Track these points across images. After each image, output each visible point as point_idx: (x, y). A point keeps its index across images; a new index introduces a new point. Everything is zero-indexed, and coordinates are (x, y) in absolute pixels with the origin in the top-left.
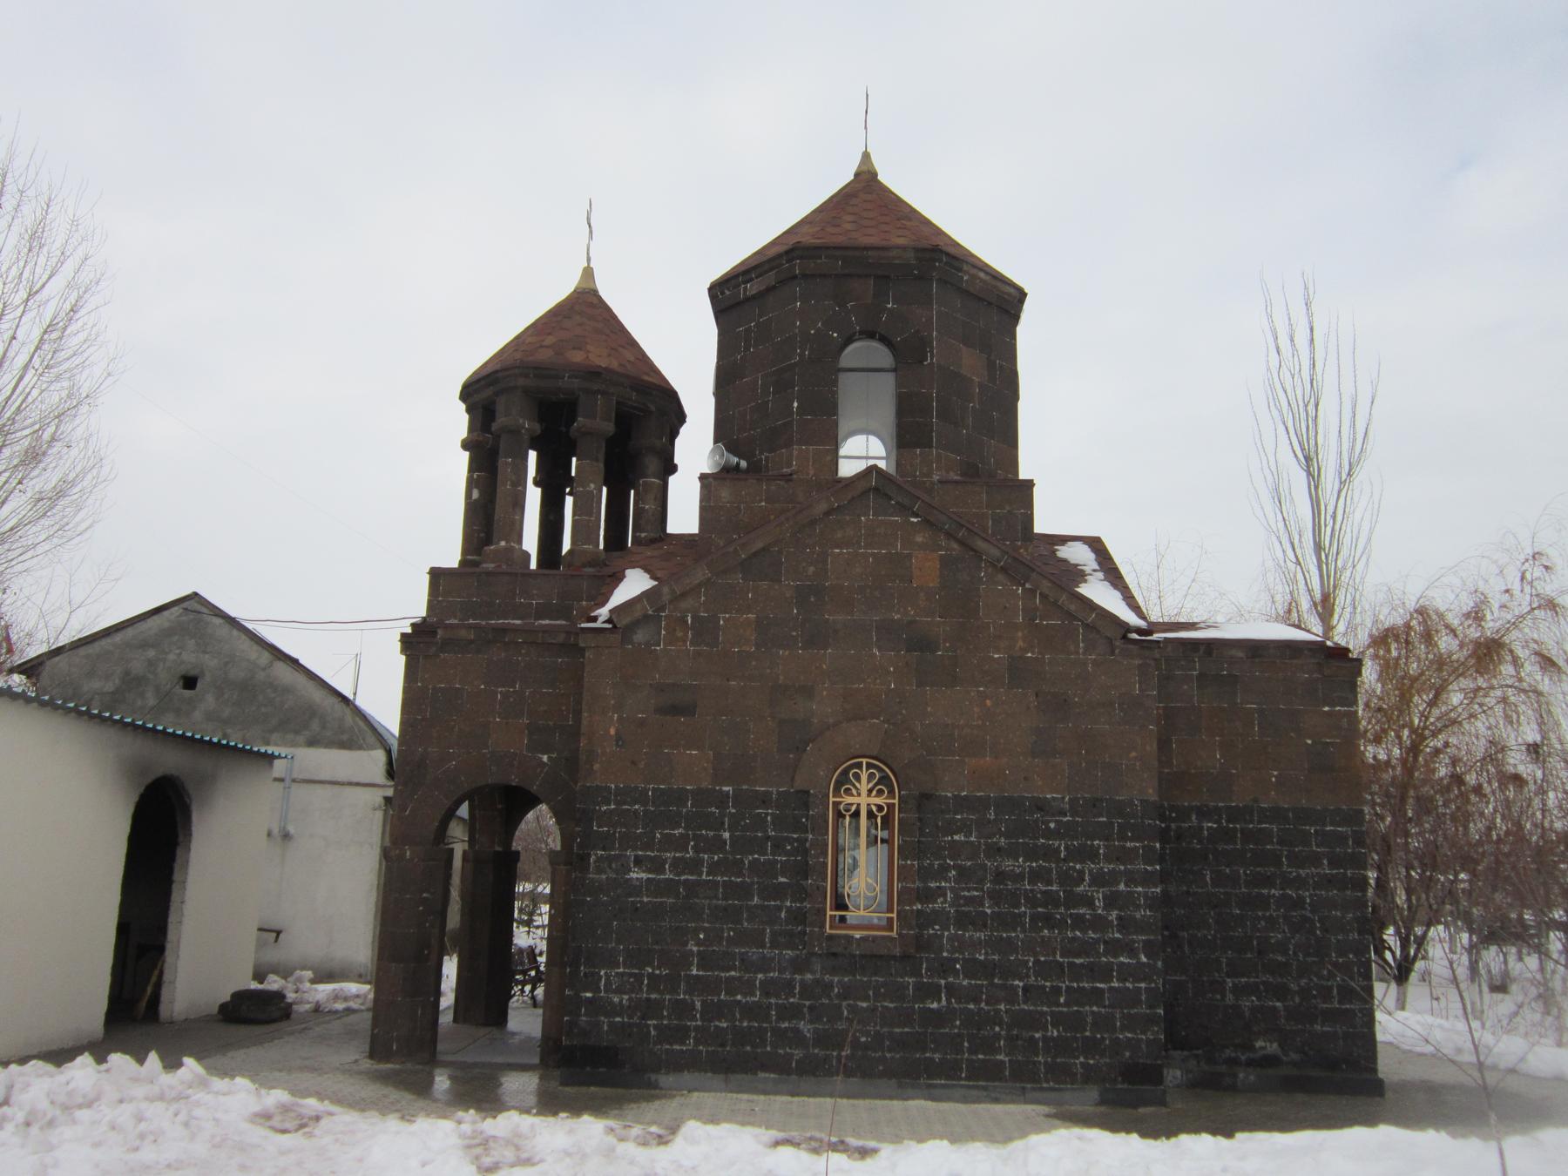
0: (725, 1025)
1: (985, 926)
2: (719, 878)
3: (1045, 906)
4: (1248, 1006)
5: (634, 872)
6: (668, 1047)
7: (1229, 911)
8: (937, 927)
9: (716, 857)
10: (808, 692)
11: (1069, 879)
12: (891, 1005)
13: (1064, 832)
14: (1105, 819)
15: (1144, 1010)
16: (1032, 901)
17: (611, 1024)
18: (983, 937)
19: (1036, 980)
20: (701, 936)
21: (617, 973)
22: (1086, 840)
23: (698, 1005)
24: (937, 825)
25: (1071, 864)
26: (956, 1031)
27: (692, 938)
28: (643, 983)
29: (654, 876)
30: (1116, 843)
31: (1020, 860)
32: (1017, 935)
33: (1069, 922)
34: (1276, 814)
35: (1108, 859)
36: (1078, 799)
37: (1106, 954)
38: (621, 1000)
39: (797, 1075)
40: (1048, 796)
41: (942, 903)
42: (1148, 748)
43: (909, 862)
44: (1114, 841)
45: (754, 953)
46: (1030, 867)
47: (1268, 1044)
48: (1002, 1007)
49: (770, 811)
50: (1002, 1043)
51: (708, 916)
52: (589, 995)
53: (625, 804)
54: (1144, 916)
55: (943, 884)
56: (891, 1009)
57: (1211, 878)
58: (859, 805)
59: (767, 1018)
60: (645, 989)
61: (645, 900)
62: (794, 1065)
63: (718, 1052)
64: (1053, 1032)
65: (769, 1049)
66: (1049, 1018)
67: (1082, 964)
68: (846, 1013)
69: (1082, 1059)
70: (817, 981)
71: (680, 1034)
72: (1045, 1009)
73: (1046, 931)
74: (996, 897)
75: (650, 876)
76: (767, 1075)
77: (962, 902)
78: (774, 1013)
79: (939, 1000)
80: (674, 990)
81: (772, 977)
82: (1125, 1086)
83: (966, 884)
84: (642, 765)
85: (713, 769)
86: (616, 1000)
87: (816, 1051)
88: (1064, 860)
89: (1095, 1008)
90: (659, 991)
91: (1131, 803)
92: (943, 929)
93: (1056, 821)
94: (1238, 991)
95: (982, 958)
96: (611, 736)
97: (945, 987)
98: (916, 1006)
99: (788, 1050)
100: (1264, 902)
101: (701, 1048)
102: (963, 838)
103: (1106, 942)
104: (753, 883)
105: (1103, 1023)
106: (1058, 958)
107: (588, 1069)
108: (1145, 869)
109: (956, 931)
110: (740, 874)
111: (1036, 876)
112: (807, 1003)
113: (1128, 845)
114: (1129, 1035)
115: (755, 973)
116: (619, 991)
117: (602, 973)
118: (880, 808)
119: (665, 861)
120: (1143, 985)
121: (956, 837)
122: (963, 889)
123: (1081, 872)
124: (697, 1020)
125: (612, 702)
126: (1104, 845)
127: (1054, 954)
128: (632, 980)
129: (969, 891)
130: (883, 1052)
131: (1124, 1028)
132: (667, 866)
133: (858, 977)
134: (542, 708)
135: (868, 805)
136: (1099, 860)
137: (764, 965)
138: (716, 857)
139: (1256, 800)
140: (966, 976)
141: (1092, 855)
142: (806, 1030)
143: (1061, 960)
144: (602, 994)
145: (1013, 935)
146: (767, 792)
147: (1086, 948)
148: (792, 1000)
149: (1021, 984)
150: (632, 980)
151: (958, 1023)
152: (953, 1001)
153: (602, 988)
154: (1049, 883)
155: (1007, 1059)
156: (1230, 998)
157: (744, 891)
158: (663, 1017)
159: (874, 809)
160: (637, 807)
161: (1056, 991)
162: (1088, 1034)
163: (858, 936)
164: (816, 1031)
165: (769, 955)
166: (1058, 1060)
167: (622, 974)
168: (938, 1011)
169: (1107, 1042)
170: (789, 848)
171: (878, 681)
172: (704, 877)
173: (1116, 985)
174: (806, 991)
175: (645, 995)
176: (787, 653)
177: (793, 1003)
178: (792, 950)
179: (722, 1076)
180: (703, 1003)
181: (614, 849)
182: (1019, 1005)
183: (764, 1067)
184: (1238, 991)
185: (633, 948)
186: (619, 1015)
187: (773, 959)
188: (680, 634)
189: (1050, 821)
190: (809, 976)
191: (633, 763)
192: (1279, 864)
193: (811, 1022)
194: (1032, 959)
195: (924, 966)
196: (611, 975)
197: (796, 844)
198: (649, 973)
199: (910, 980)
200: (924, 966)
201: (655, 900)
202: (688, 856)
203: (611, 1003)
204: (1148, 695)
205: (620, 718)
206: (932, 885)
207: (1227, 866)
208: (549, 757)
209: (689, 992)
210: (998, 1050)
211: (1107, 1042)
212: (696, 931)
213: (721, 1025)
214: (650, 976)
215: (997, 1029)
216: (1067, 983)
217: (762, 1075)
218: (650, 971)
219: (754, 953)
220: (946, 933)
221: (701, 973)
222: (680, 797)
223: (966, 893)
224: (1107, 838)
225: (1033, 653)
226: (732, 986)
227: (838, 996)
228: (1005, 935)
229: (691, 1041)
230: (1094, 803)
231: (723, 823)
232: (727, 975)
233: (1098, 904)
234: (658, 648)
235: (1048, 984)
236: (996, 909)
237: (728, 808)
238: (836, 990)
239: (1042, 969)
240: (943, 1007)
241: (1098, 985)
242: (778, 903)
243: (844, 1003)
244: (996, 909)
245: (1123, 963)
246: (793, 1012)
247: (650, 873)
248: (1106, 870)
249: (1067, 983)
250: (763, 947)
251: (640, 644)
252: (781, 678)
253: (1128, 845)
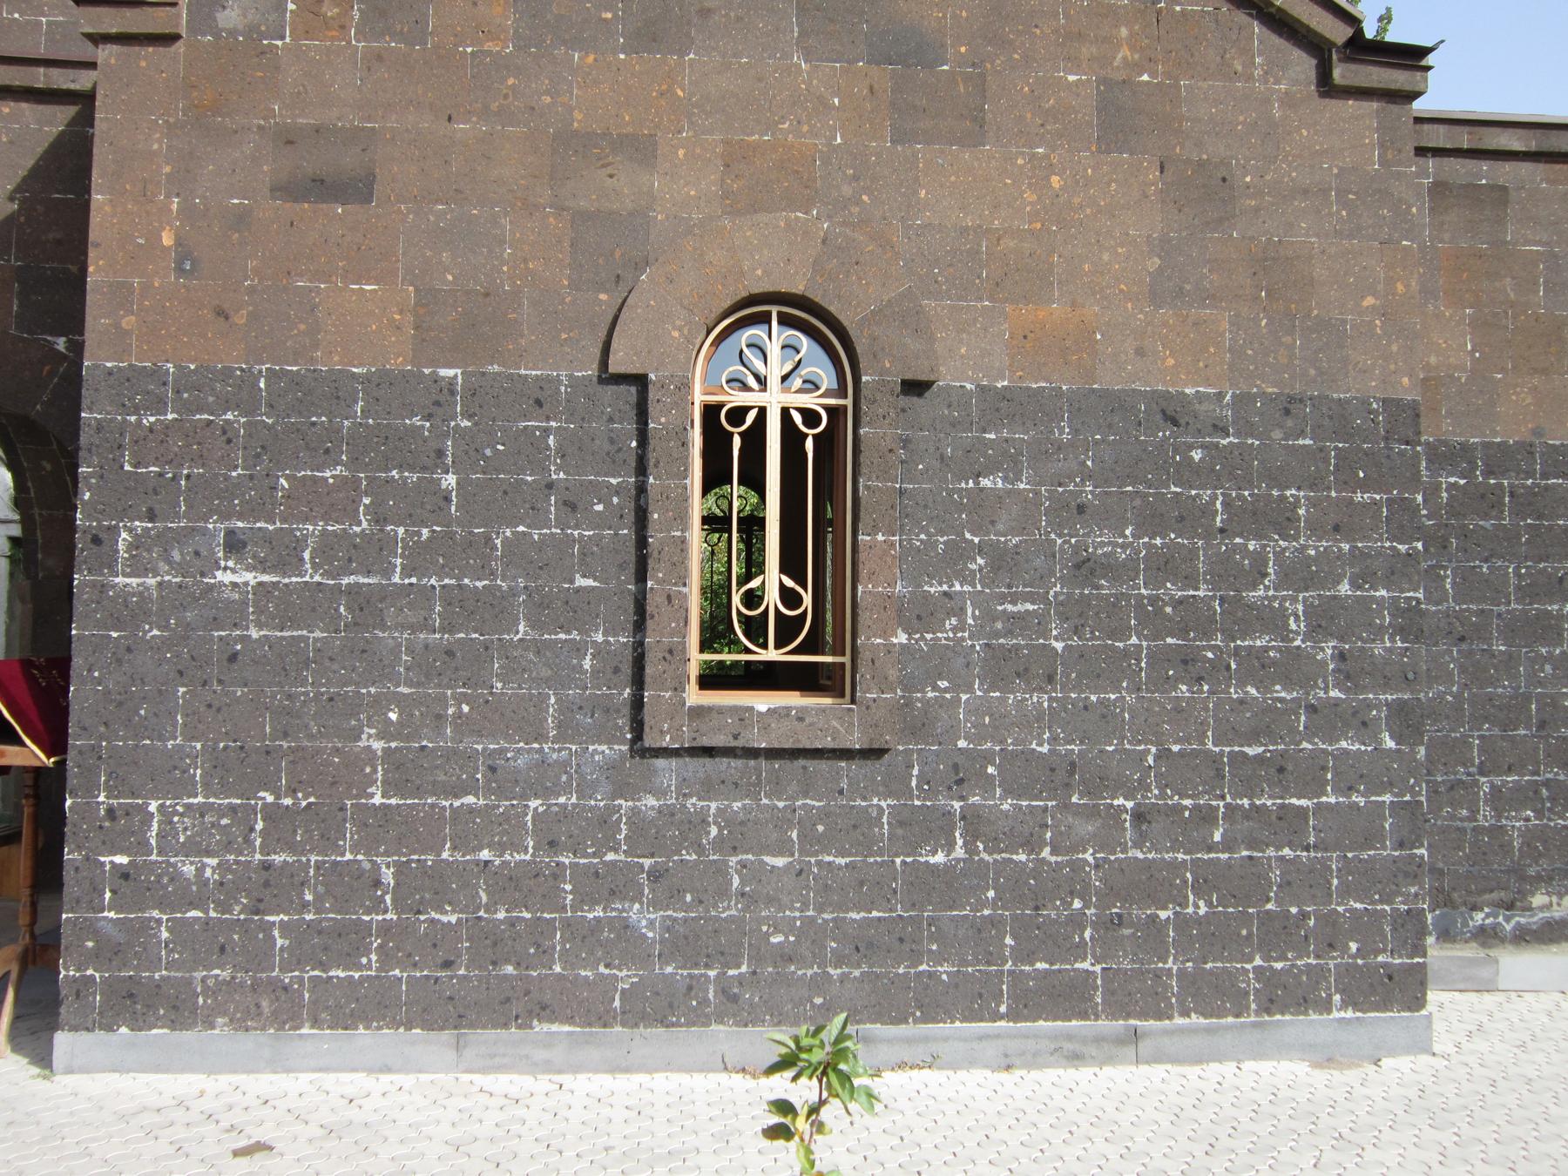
0: (453, 919)
1: (1050, 679)
2: (433, 581)
3: (1182, 632)
4: (1519, 829)
5: (226, 568)
6: (316, 973)
7: (1485, 647)
8: (943, 684)
9: (425, 532)
10: (642, 150)
12: (842, 861)
13: (1225, 468)
14: (1308, 442)
15: (1389, 852)
16: (1152, 620)
17: (177, 927)
18: (1046, 704)
19: (1162, 796)
20: (393, 716)
21: (188, 807)
22: (1270, 487)
23: (388, 876)
24: (942, 457)
25: (1238, 540)
26: (986, 912)
27: (369, 719)
28: (252, 829)
29: (275, 579)
30: (1333, 494)
31: (1128, 532)
32: (1121, 696)
33: (1233, 666)
35: (1315, 529)
36: (1251, 398)
37: (1310, 731)
38: (200, 870)
39: (623, 1025)
40: (1187, 391)
41: (955, 629)
42: (1400, 287)
43: (880, 537)
44: (1329, 489)
45: (520, 754)
46: (1148, 546)
47: (1555, 899)
48: (1088, 857)
49: (553, 424)
50: (1087, 934)
51: (407, 669)
52: (122, 859)
53: (200, 410)
54: (1389, 650)
55: (958, 587)
56: (840, 867)
57: (1454, 584)
58: (762, 412)
59: (552, 899)
60: (258, 842)
61: (254, 633)
62: (617, 1003)
63: (437, 980)
64: (1197, 906)
65: (558, 969)
66: (1188, 875)
67: (1259, 759)
68: (736, 882)
69: (1258, 961)
70: (667, 813)
72: (1180, 856)
73: (1184, 688)
74: (1075, 615)
75: (266, 578)
76: (555, 1027)
77: (999, 625)
78: (568, 887)
79: (950, 846)
80: (329, 842)
81: (564, 806)
82: (1349, 1014)
83: (1010, 586)
84: (240, 319)
85: (416, 328)
86: (189, 870)
87: (669, 970)
88: (1222, 531)
89: (1286, 851)
90: (292, 847)
91: (1365, 402)
92: (956, 688)
93: (1203, 446)
95: (1045, 749)
96: (166, 249)
97: (963, 818)
98: (898, 861)
99: (602, 969)
101: (397, 972)
102: (1000, 485)
103: (1312, 709)
104: (513, 592)
106: (1210, 745)
107: (124, 1030)
108: (1393, 548)
109: (986, 691)
110: (484, 571)
111: (1164, 566)
112: (647, 862)
113: (1358, 497)
114: (1358, 906)
115: (524, 797)
116: (194, 849)
117: (153, 806)
118: (810, 417)
119: (300, 544)
120: (1387, 798)
121: (986, 482)
122: (1003, 599)
123: (1259, 560)
124: (386, 911)
125: (167, 169)
126: (1307, 498)
127: (1201, 739)
128: (225, 821)
129: (1014, 603)
130: (822, 965)
131: (1346, 892)
132: (307, 555)
133: (765, 801)
134: (51, 236)
135: (785, 412)
136: (1297, 529)
137: (543, 780)
138: (425, 532)
139: (1537, 432)
140: (1008, 792)
141: (1283, 522)
142: (644, 923)
143: (1217, 749)
144: (154, 857)
145: (1113, 697)
146: (548, 379)
147: (1267, 724)
148: (610, 857)
149: (1130, 805)
150: (225, 821)
151: (991, 894)
152: (981, 847)
153: (153, 842)
154: (1191, 581)
155: (1098, 968)
156: (1485, 816)
157: (495, 609)
158: (305, 906)
159: (797, 418)
160: (229, 416)
161: (1206, 817)
162: (1269, 906)
163: (763, 708)
164: (669, 926)
165: (555, 756)
166: (1209, 966)
167: (203, 810)
168: (948, 868)
169: (1312, 923)
170: (599, 508)
171: (805, 128)
172: (396, 579)
173: (1332, 800)
174: (645, 835)
175: (258, 856)
176: (591, 58)
177: (614, 863)
178: (609, 742)
179: (447, 1035)
180: (401, 870)
181: (177, 516)
182: (1124, 851)
183: (545, 1011)
185: (226, 748)
186: (192, 905)
187: (564, 765)
188: (332, 12)
189: (1191, 447)
190: (651, 801)
191: (222, 314)
193: (655, 904)
194: (1153, 750)
195: (915, 772)
196: (176, 813)
197: (615, 500)
198: (265, 805)
199: (883, 804)
200: (915, 772)
201: (279, 634)
202: (357, 529)
203: (176, 877)
204: (1399, 173)
205: (187, 211)
206: (932, 590)
207: (1486, 560)
208: (69, 341)
209: (367, 844)
210: (1079, 951)
211: (1312, 923)
212: (378, 705)
213: (445, 919)
214: (271, 813)
215: (1077, 904)
216: (1228, 799)
217: (540, 1027)
218: (270, 799)
219: (520, 754)
220: (964, 697)
221: (393, 801)
222: (337, 391)
223: (1010, 607)
225: (1153, 74)
226: (467, 830)
227: (719, 843)
228: (1093, 698)
229: (374, 957)
230: (1288, 405)
231: (440, 453)
232: (457, 804)
233: (1293, 626)
234: (279, 43)
235: (1187, 802)
236: (1075, 641)
237: (454, 418)
238: (714, 831)
239: (1176, 770)
240: (958, 860)
241: (1294, 801)
242: (575, 635)
243: (733, 861)
244: (1075, 641)
245: (1346, 752)
246: (614, 885)
247: (264, 571)
248: (1312, 553)
249: (1228, 799)
250: (541, 737)
251: (233, 33)
252: (577, 115)
253: (1358, 497)
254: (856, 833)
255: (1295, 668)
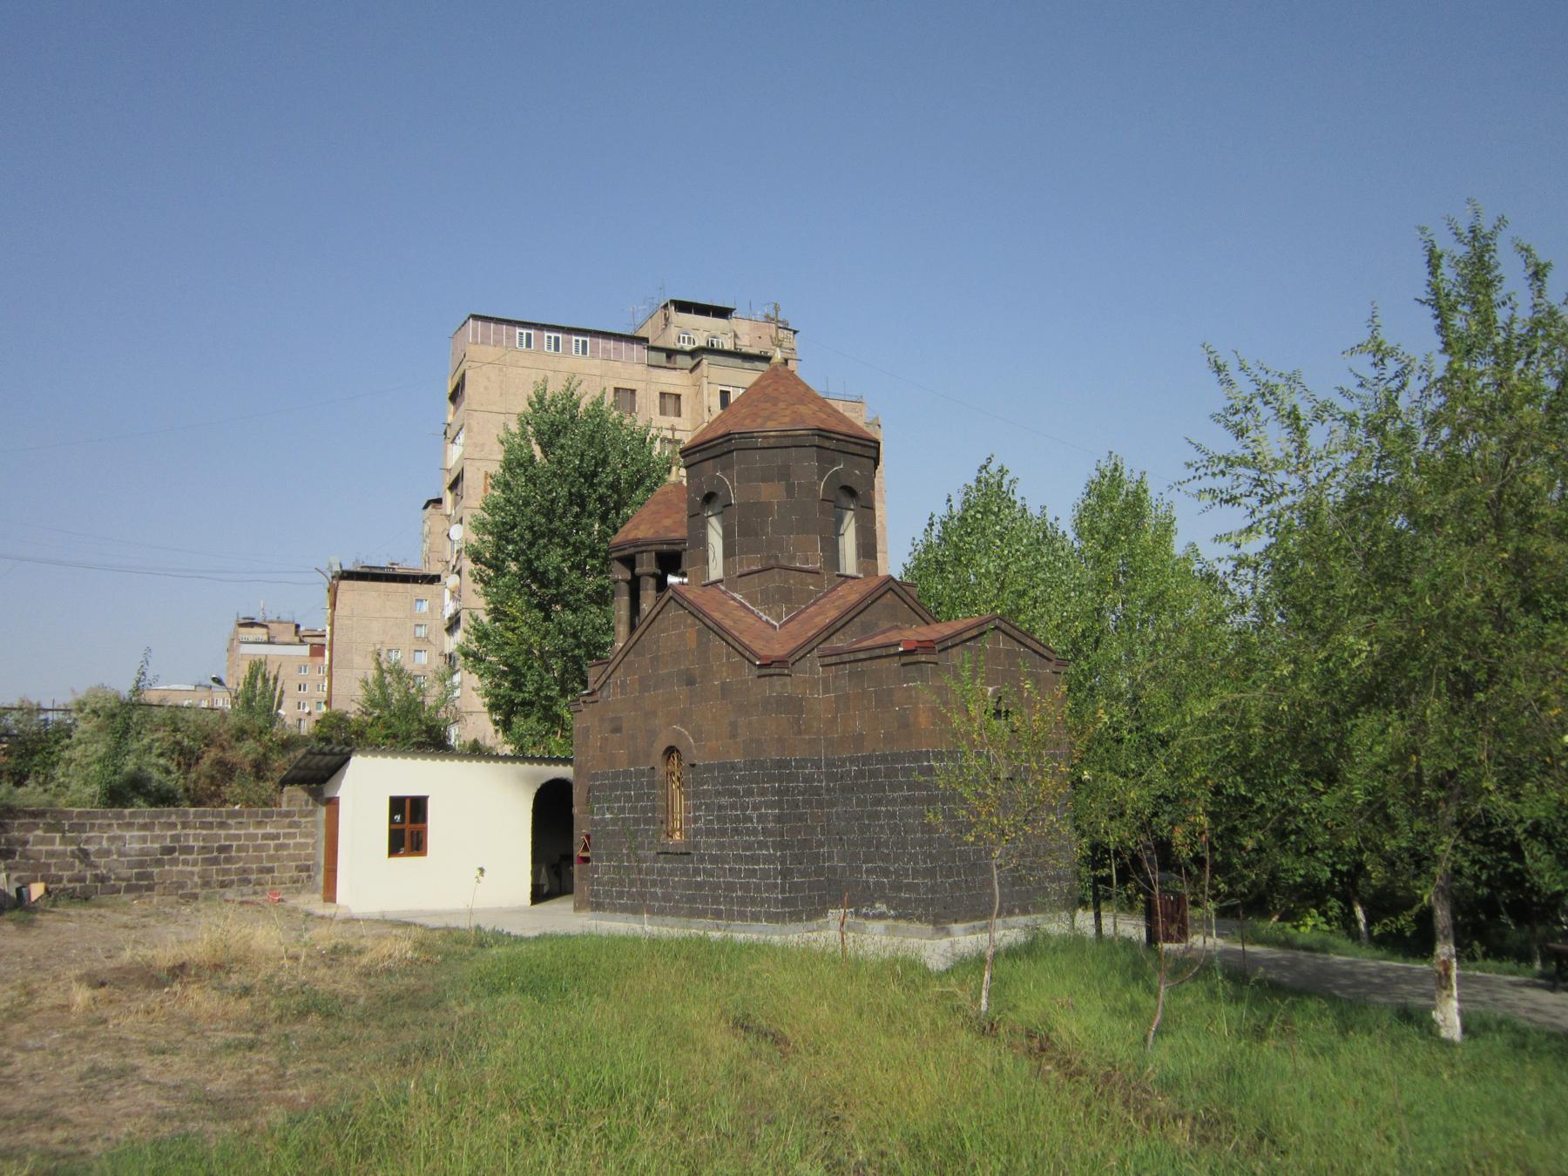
11: (744, 808)
34: (883, 759)
35: (758, 795)
71: (620, 895)
74: (720, 819)
94: (868, 871)
100: (875, 816)
105: (757, 888)
147: (749, 847)
184: (868, 871)
192: (884, 791)
210: (720, 904)
224: (757, 783)
246: (654, 883)
254: (685, 872)
255: (754, 832)
